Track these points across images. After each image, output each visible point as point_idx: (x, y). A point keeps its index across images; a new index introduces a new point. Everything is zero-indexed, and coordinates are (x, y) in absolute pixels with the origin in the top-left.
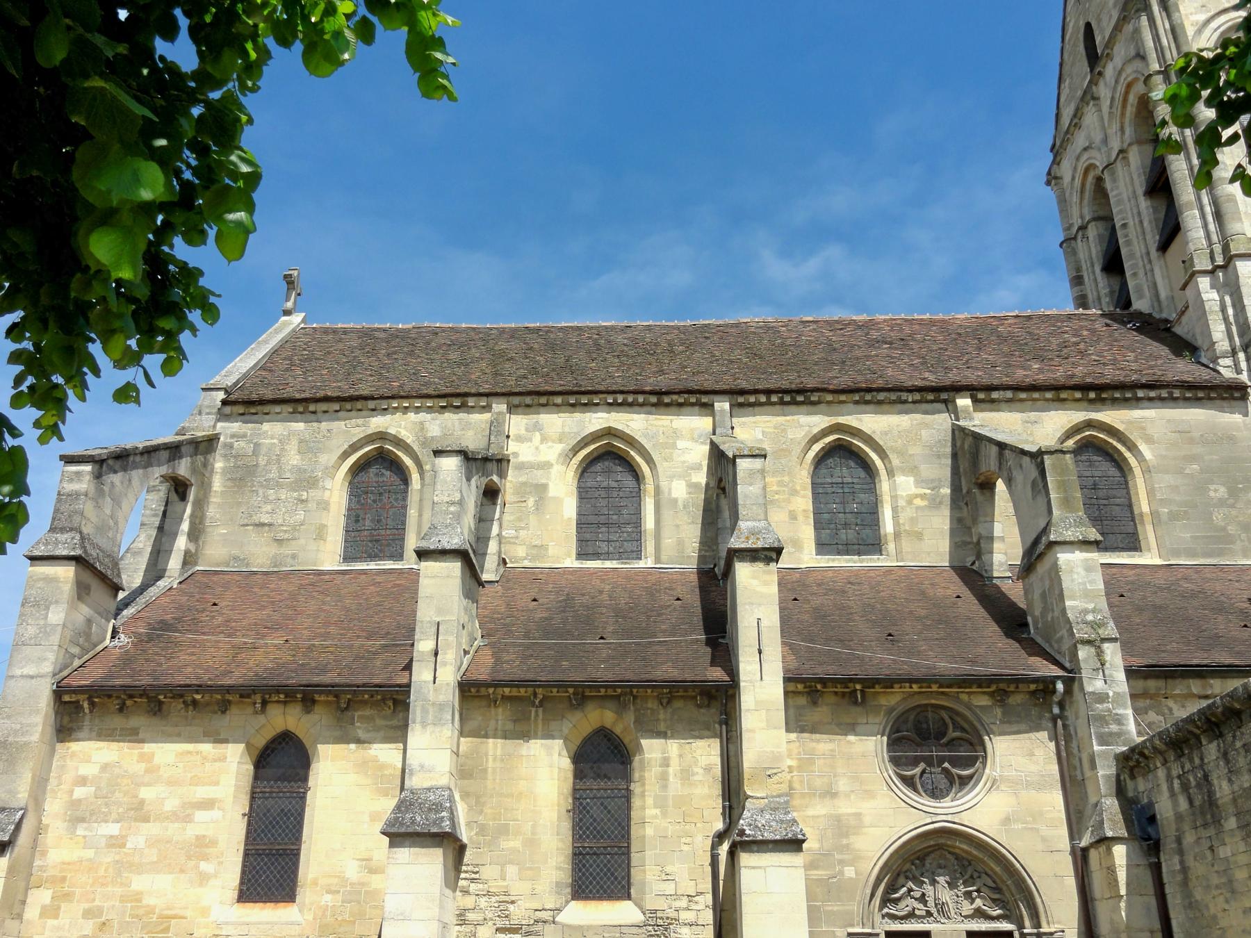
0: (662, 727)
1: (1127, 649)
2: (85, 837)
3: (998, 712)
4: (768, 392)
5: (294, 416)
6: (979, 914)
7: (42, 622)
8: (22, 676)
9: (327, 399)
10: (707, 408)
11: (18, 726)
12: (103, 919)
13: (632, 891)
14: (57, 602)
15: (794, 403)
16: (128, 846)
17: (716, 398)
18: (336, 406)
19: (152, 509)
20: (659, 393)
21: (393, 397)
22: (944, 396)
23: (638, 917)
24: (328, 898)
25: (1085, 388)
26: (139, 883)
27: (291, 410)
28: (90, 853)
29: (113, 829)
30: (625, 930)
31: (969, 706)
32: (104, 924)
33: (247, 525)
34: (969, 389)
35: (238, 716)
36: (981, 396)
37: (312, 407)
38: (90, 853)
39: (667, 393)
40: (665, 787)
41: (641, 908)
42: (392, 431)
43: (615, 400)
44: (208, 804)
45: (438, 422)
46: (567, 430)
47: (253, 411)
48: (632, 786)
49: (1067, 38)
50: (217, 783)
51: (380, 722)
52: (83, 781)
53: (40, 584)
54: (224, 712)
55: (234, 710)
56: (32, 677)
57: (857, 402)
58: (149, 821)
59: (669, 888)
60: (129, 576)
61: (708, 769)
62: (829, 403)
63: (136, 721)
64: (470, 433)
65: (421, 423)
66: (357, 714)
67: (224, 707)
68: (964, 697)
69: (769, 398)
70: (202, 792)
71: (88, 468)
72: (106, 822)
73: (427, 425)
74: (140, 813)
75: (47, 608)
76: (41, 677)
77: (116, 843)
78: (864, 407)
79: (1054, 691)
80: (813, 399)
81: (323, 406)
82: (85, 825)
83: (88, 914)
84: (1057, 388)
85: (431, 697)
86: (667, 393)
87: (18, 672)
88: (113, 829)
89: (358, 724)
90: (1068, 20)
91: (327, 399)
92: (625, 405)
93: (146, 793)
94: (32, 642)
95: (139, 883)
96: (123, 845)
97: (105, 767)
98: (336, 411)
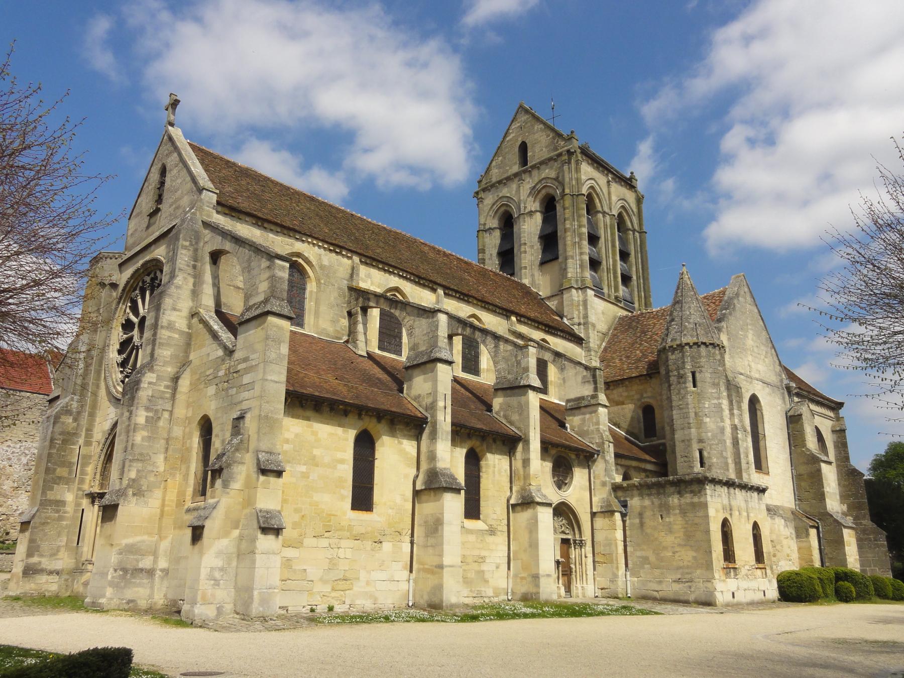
0: (493, 452)
1: (615, 446)
2: (291, 471)
3: (577, 461)
4: (456, 292)
5: (255, 225)
6: (563, 532)
7: (278, 351)
8: (271, 380)
9: (276, 224)
10: (434, 290)
11: (272, 409)
12: (303, 514)
13: (481, 516)
14: (284, 342)
15: (463, 300)
16: (311, 478)
17: (439, 287)
18: (279, 230)
19: (185, 261)
20: (420, 277)
21: (310, 236)
22: (508, 314)
23: (486, 528)
24: (390, 511)
25: (546, 325)
26: (317, 497)
27: (254, 222)
28: (294, 480)
29: (303, 468)
30: (484, 532)
31: (570, 457)
32: (303, 516)
33: (230, 286)
34: (517, 315)
35: (351, 419)
36: (518, 318)
37: (266, 225)
38: (294, 480)
39: (423, 279)
40: (494, 476)
41: (486, 524)
42: (306, 255)
43: (406, 276)
44: (342, 461)
45: (327, 257)
46: (382, 282)
47: (233, 214)
48: (481, 474)
49: (508, 139)
50: (345, 452)
51: (406, 433)
52: (287, 441)
53: (275, 329)
54: (346, 416)
55: (350, 415)
56: (276, 382)
57: (482, 307)
58: (318, 466)
59: (495, 517)
60: (174, 301)
61: (506, 471)
62: (473, 304)
63: (309, 413)
64: (341, 269)
65: (320, 255)
66: (397, 427)
67: (346, 413)
68: (570, 454)
69: (468, 299)
70: (339, 455)
71: (287, 265)
72: (300, 464)
73: (322, 257)
74: (314, 462)
75: (280, 344)
76: (281, 383)
77: (305, 476)
78: (483, 309)
79: (594, 457)
80: (470, 300)
81: (273, 227)
82: (290, 465)
83: (297, 511)
84: (539, 323)
85: (444, 428)
86: (423, 279)
87: (269, 378)
88: (303, 468)
89: (398, 432)
90: (511, 131)
91: (276, 224)
92: (405, 278)
93: (316, 452)
94: (274, 362)
95: (317, 497)
96: (308, 477)
97: (297, 435)
98: (278, 232)
